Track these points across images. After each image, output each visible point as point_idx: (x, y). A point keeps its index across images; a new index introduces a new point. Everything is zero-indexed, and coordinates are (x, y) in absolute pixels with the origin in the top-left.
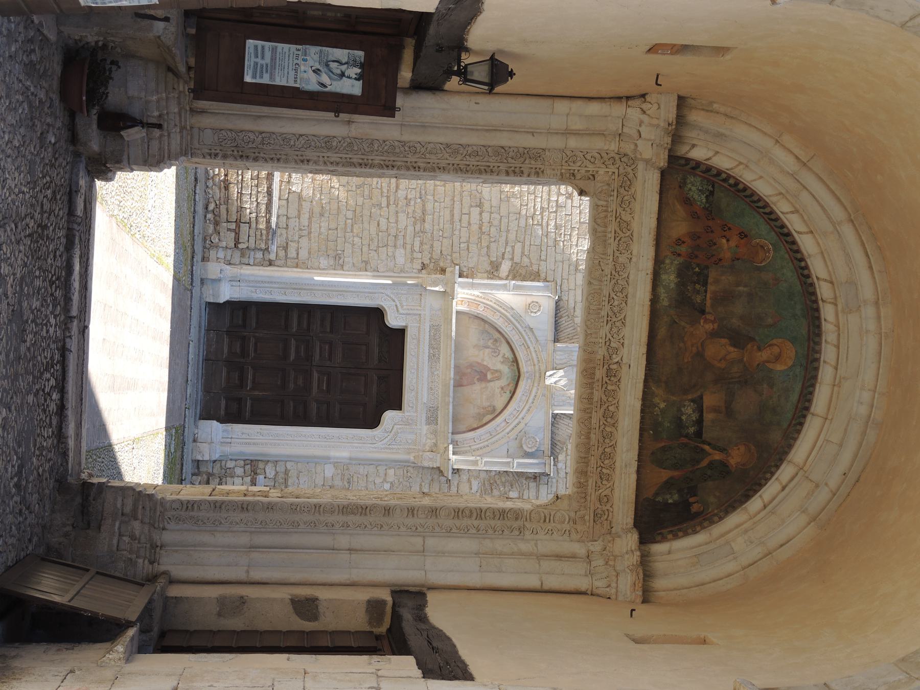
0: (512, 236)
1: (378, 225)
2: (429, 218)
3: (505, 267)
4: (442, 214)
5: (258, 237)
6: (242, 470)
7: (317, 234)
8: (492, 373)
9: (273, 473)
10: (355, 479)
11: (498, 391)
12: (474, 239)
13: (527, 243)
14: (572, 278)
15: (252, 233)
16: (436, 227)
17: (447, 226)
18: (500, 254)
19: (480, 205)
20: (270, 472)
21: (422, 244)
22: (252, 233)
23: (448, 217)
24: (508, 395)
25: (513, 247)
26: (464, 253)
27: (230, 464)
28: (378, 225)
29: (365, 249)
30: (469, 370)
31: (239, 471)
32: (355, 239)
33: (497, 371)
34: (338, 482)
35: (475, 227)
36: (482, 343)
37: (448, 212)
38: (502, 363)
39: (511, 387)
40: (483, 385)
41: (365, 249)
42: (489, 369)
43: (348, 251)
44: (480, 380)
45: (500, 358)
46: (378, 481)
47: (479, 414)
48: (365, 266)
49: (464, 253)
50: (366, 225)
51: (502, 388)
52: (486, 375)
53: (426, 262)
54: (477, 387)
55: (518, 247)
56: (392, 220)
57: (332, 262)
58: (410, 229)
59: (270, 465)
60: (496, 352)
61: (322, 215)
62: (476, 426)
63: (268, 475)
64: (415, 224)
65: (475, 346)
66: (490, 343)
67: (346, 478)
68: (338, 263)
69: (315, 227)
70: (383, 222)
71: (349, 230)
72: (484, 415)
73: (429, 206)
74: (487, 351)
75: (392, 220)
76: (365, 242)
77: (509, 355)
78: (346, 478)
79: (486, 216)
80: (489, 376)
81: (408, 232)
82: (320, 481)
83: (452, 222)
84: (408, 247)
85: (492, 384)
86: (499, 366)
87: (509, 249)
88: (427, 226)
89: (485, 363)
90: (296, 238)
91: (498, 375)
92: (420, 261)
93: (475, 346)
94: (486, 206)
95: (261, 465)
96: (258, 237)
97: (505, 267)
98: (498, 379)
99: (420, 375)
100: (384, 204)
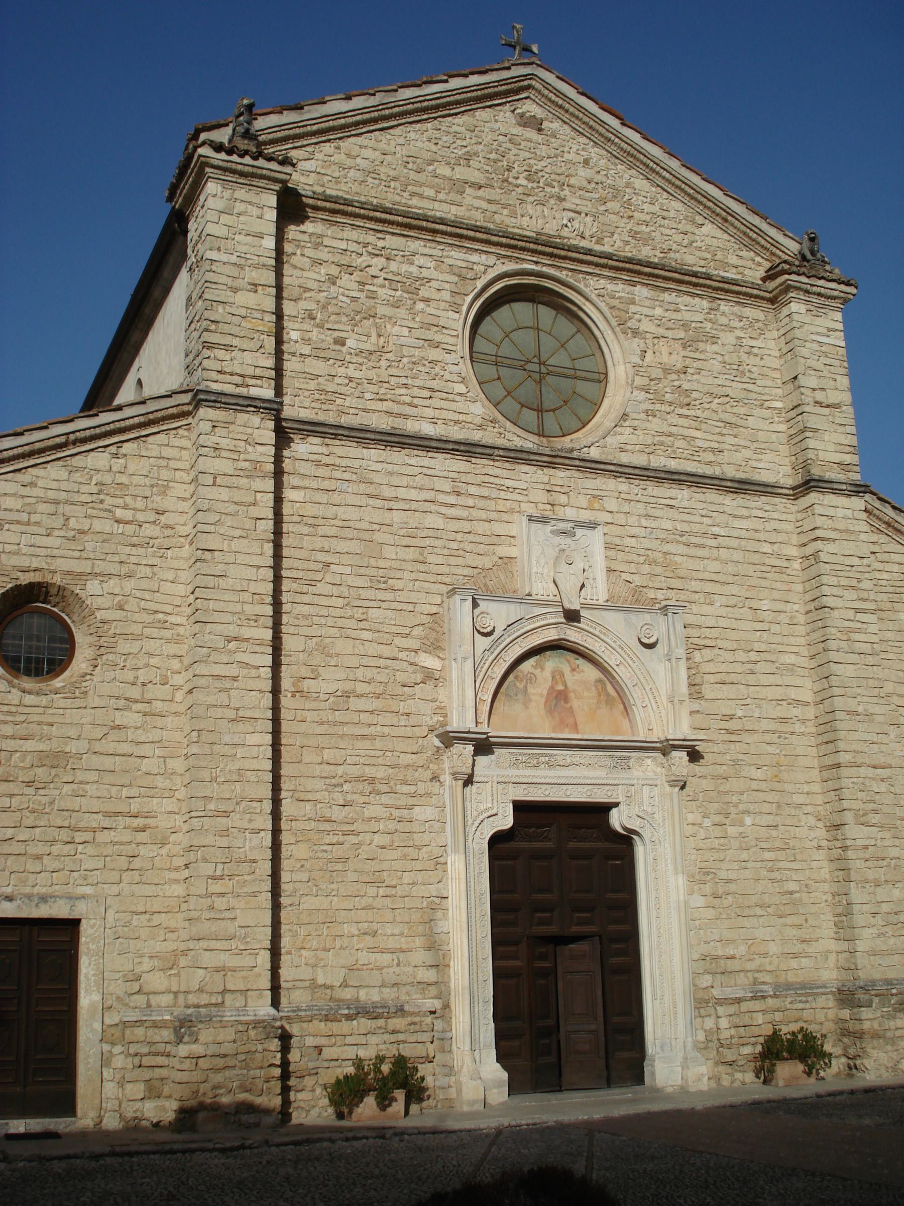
0: (386, 651)
1: (383, 847)
2: (369, 771)
3: (430, 661)
4: (362, 753)
5: (417, 1027)
6: (706, 1019)
7: (403, 940)
8: (557, 683)
9: (708, 977)
10: (703, 865)
11: (577, 676)
12: (394, 705)
13: (394, 629)
14: (435, 569)
15: (412, 1038)
16: (380, 761)
17: (378, 744)
18: (411, 669)
19: (347, 695)
20: (706, 981)
21: (405, 783)
22: (412, 1038)
23: (367, 744)
24: (581, 662)
25: (401, 649)
26: (413, 720)
27: (701, 1037)
28: (383, 847)
29: (418, 865)
30: (556, 714)
31: (709, 1023)
32: (406, 881)
33: (553, 677)
34: (708, 889)
35: (376, 704)
36: (520, 696)
37: (360, 744)
38: (543, 669)
39: (571, 656)
40: (572, 695)
41: (418, 865)
42: (552, 688)
43: (423, 891)
44: (566, 700)
45: (537, 672)
46: (702, 834)
47: (607, 702)
48: (439, 864)
49: (413, 720)
50: (385, 866)
51: (573, 670)
52: (560, 693)
53: (428, 774)
54: (575, 703)
55: (398, 641)
56: (374, 826)
57: (439, 914)
58: (385, 799)
59: (698, 982)
60: (531, 679)
61: (375, 934)
62: (621, 706)
63: (709, 984)
64: (379, 793)
65: (526, 705)
66: (520, 686)
67: (703, 878)
68: (436, 905)
69: (392, 944)
70: (378, 839)
71: (393, 891)
72: (608, 695)
73: (355, 771)
74: (530, 690)
75: (374, 826)
76: (409, 865)
77: (531, 662)
78: (703, 878)
79: (361, 688)
80: (560, 687)
81: (390, 802)
82: (710, 913)
83: (372, 737)
84: (411, 801)
85: (569, 684)
86: (547, 673)
87: (402, 655)
88: (380, 773)
89: (545, 692)
90: (410, 970)
91: (558, 675)
92: (429, 783)
93: (526, 705)
94: (348, 686)
95: (700, 995)
96: (417, 1027)
97: (430, 661)
98: (562, 675)
99: (569, 780)
100: (353, 839)
